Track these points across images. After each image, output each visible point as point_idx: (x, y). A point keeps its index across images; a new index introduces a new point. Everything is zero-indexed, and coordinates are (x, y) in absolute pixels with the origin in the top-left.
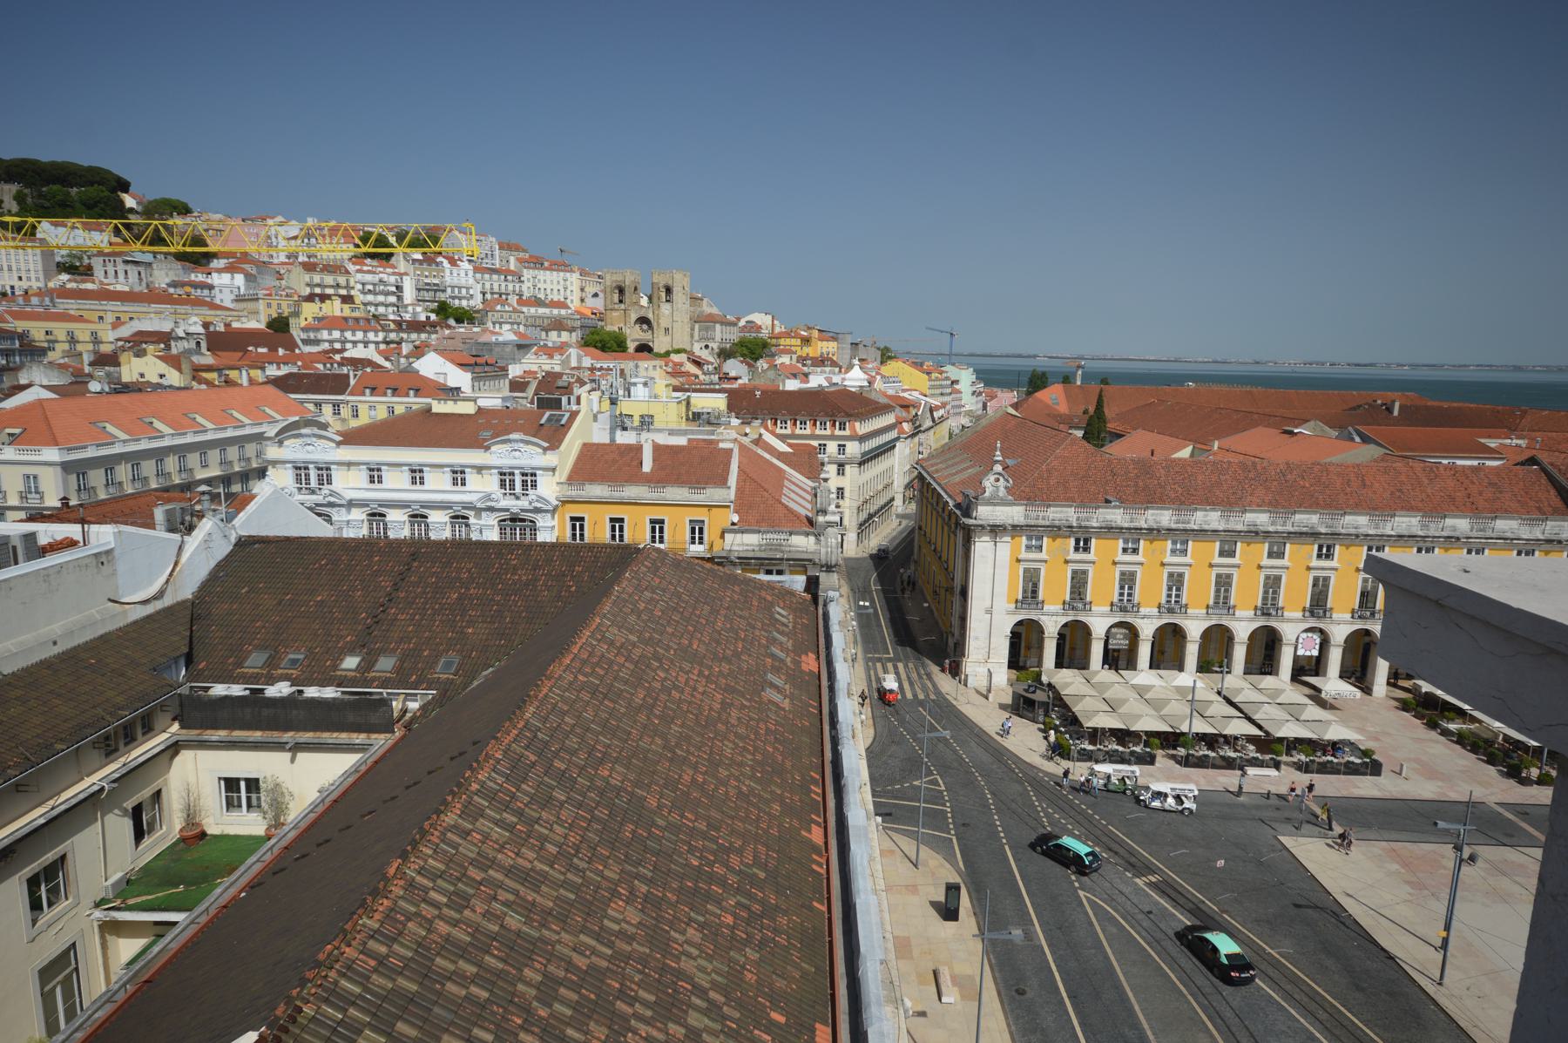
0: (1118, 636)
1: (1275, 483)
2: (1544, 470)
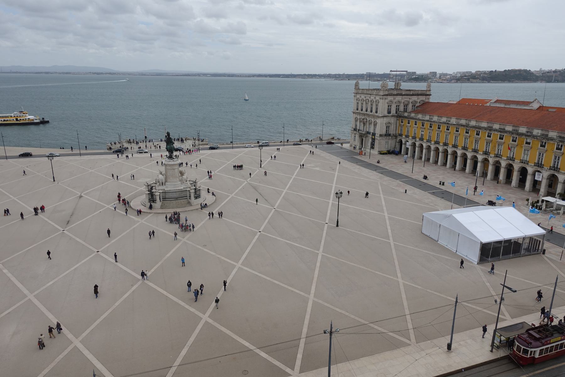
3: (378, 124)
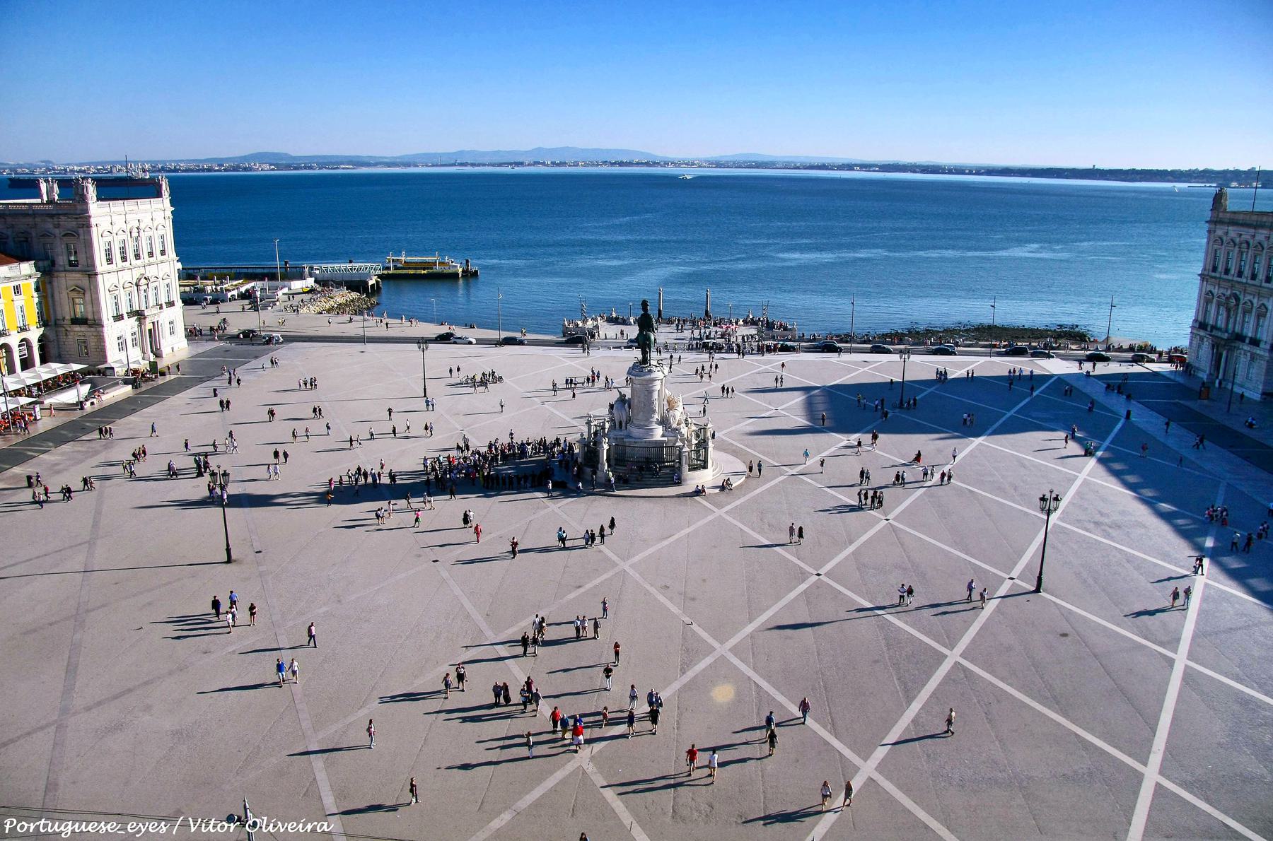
3: (1268, 314)
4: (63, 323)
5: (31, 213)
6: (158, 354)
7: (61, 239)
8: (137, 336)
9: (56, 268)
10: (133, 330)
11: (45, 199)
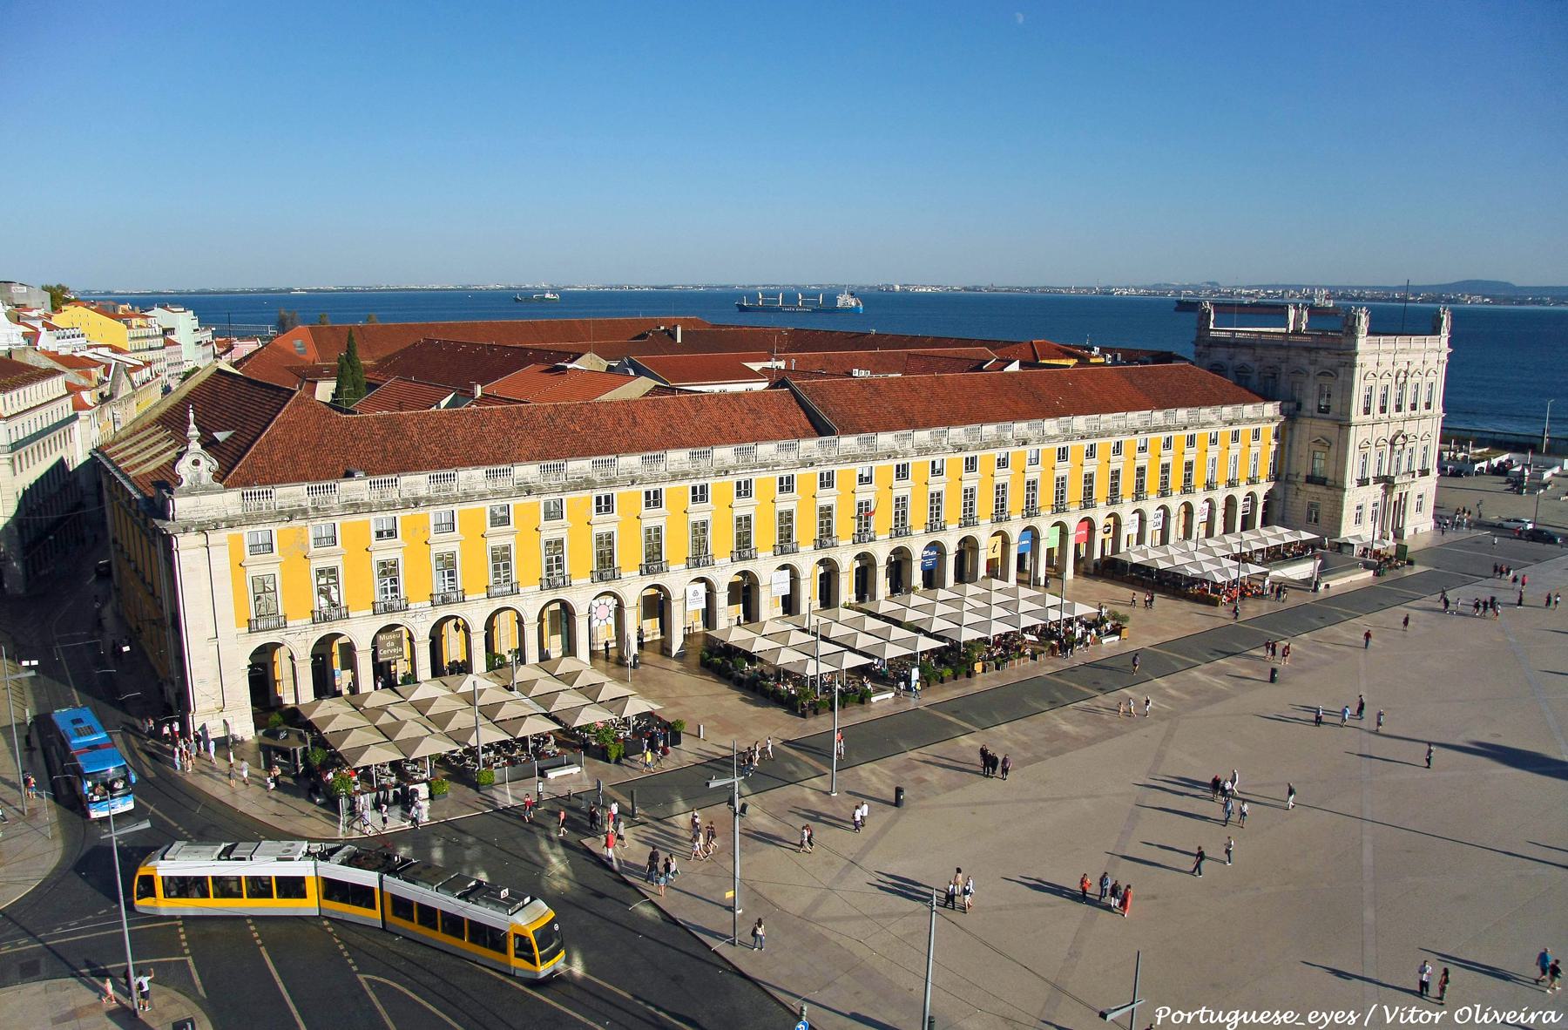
0: (388, 644)
1: (544, 430)
2: (793, 391)
4: (1295, 479)
5: (1282, 345)
6: (1399, 534)
7: (1314, 377)
8: (1378, 508)
9: (1302, 413)
10: (1376, 500)
11: (1291, 328)
